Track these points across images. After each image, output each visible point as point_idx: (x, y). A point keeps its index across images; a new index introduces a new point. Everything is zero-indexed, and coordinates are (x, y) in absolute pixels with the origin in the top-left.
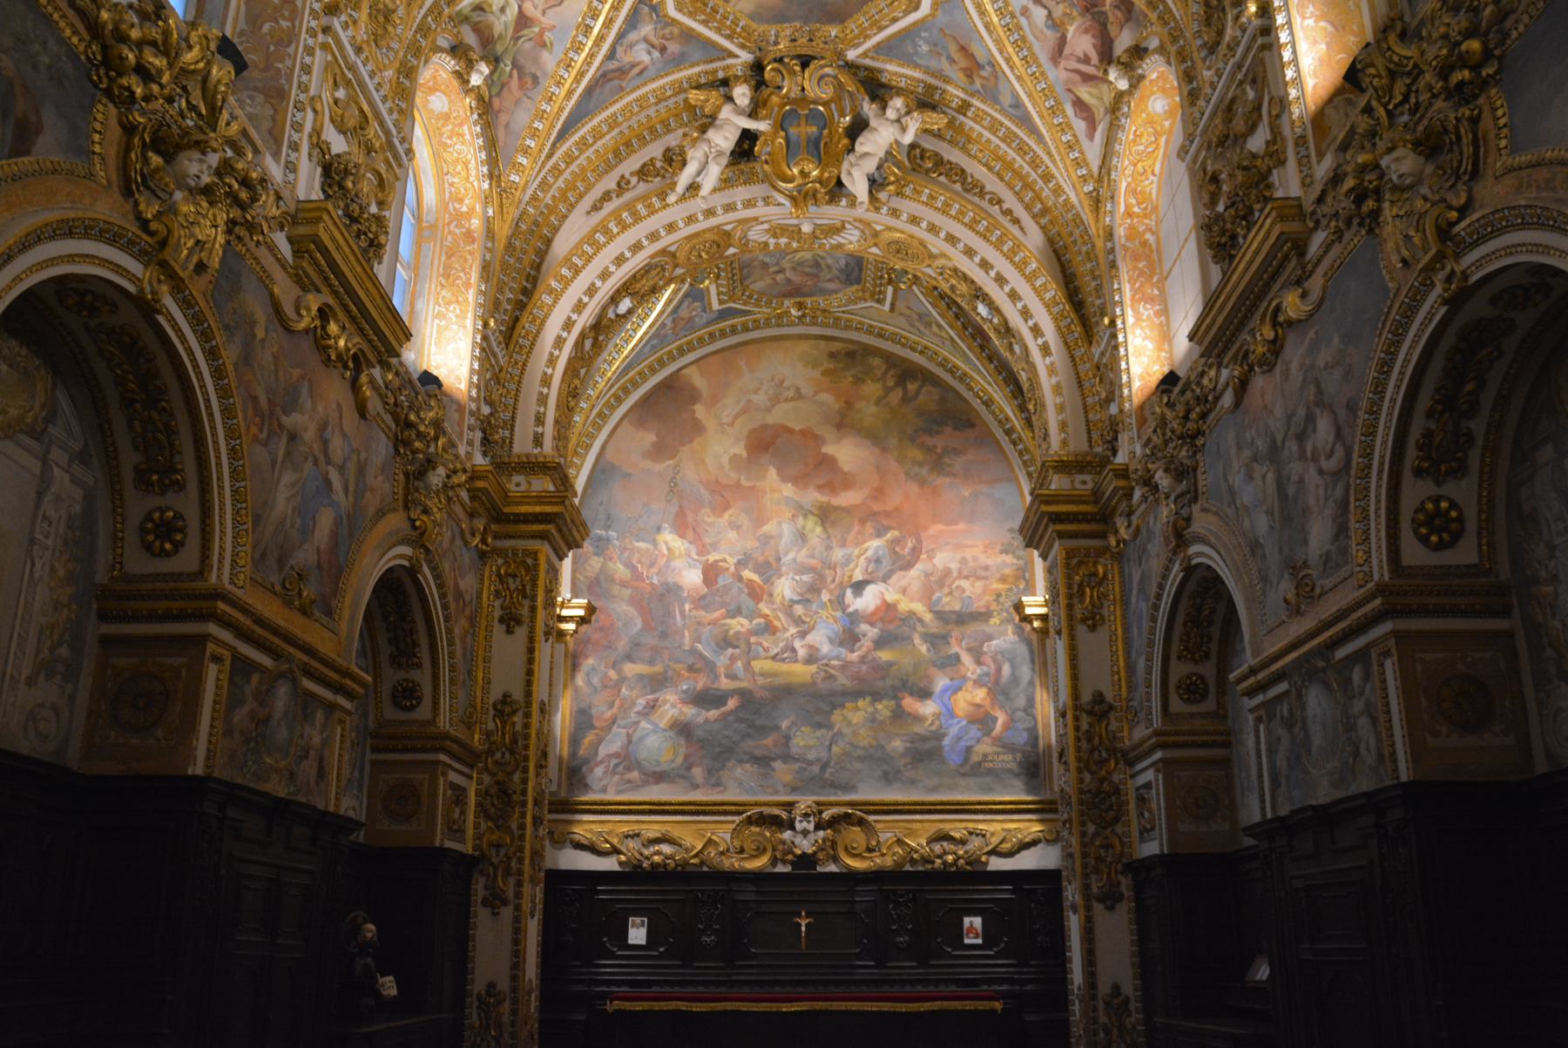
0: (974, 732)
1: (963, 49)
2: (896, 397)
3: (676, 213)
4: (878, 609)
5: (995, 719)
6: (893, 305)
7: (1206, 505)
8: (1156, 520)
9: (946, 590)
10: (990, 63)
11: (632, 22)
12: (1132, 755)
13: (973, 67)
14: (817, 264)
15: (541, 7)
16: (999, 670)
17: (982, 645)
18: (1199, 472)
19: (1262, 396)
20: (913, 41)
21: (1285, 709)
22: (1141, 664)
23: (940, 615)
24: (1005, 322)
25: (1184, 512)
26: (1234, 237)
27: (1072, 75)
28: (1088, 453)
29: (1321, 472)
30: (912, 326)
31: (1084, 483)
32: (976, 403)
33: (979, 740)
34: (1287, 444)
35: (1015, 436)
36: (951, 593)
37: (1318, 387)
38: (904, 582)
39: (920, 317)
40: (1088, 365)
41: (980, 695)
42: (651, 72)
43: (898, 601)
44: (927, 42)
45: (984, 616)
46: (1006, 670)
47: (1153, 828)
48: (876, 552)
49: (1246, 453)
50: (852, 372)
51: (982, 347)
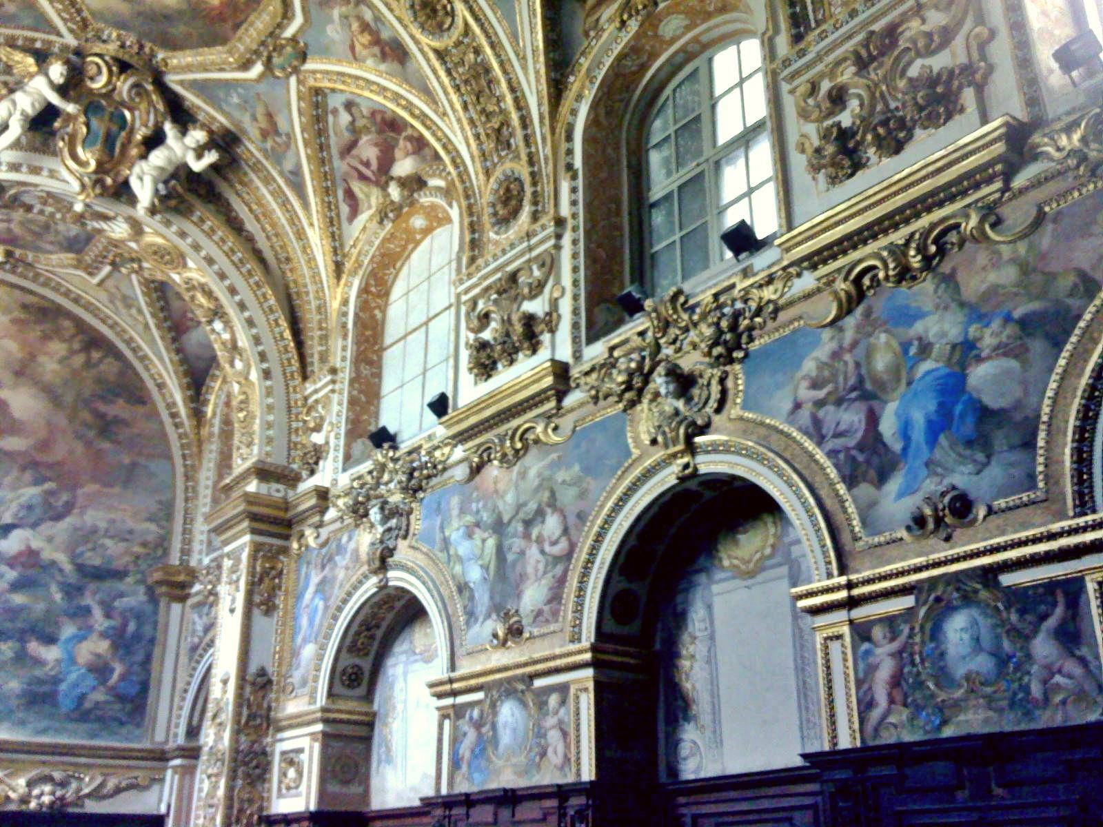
0: (91, 681)
1: (270, 116)
2: (79, 360)
4: (20, 554)
5: (112, 671)
6: (101, 283)
7: (414, 543)
8: (350, 539)
9: (90, 546)
10: (288, 136)
12: (284, 723)
13: (271, 130)
14: (47, 227)
16: (125, 625)
17: (114, 599)
18: (412, 517)
19: (495, 483)
21: (476, 713)
22: (308, 651)
23: (81, 568)
24: (234, 341)
25: (391, 544)
26: (495, 363)
28: (285, 468)
29: (542, 552)
30: (112, 302)
31: (278, 491)
32: (150, 385)
33: (94, 688)
34: (514, 524)
35: (177, 420)
36: (93, 549)
37: (553, 493)
38: (50, 532)
39: (125, 298)
40: (299, 396)
41: (103, 646)
43: (42, 549)
44: (239, 96)
45: (120, 575)
46: (132, 627)
47: (297, 787)
48: (31, 499)
49: (469, 519)
50: (42, 327)
51: (174, 340)
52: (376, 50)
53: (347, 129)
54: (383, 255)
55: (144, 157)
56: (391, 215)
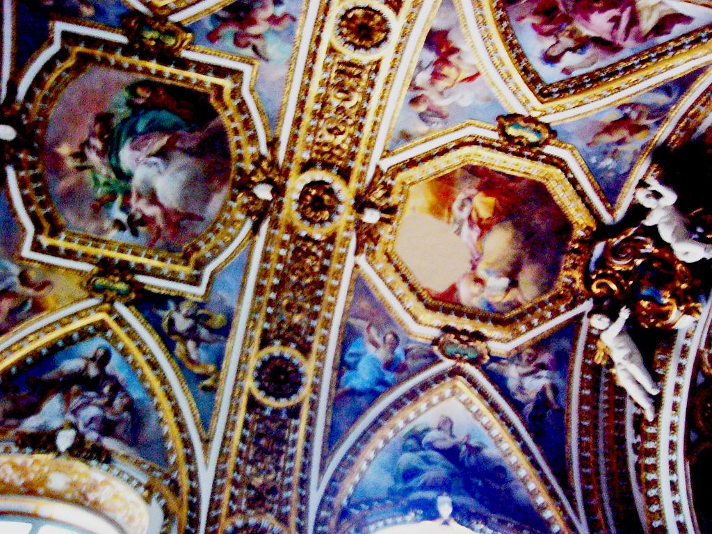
1: (609, 129)
3: (666, 415)
10: (621, 107)
11: (498, 380)
15: (447, 436)
20: (601, 171)
27: (632, 35)
42: (560, 382)
44: (602, 160)
55: (668, 245)
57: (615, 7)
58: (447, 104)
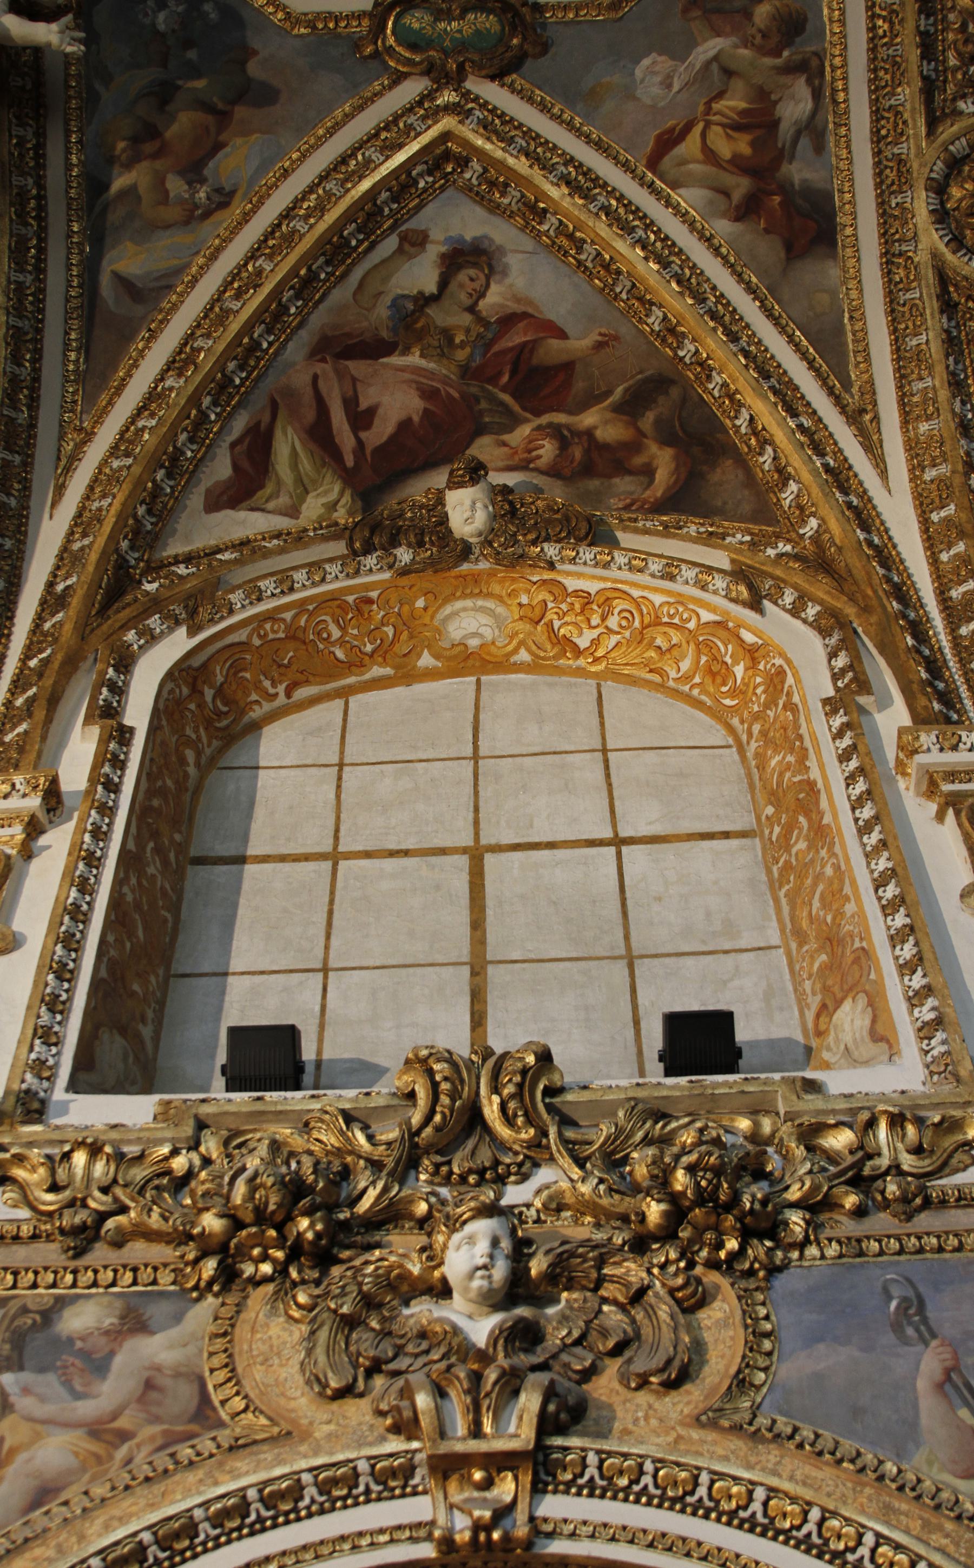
10: (223, 198)
52: (741, 186)
53: (396, 303)
54: (294, 635)
56: (404, 555)
57: (380, 450)
58: (700, 49)
